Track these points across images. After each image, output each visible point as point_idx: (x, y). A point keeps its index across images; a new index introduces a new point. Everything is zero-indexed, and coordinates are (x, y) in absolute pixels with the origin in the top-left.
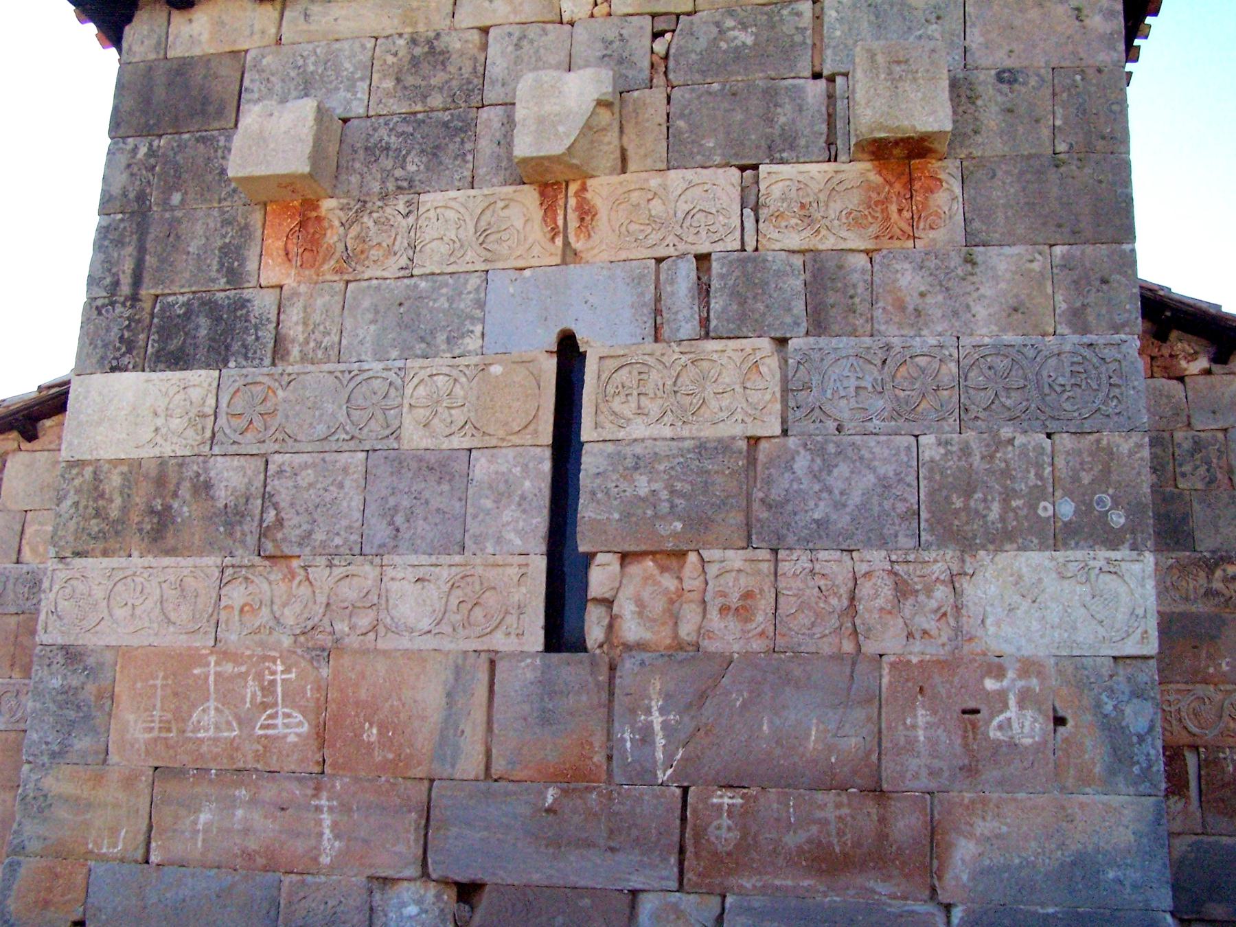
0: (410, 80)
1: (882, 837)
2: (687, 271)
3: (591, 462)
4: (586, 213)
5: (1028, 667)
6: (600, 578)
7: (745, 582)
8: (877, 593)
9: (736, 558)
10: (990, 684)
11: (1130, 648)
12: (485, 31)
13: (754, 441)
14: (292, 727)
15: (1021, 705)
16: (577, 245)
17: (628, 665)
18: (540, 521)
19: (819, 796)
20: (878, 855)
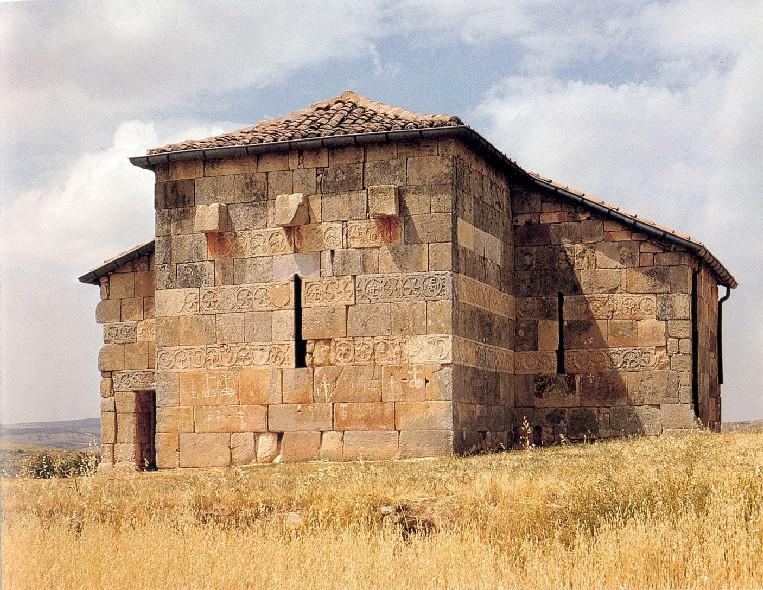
0: (246, 191)
1: (383, 414)
2: (328, 254)
3: (304, 312)
4: (300, 237)
5: (419, 368)
6: (309, 348)
7: (346, 348)
8: (380, 348)
9: (344, 340)
10: (410, 373)
11: (445, 362)
12: (267, 173)
13: (347, 307)
14: (230, 393)
15: (417, 378)
16: (299, 247)
17: (317, 370)
18: (292, 331)
19: (367, 405)
20: (382, 419)
